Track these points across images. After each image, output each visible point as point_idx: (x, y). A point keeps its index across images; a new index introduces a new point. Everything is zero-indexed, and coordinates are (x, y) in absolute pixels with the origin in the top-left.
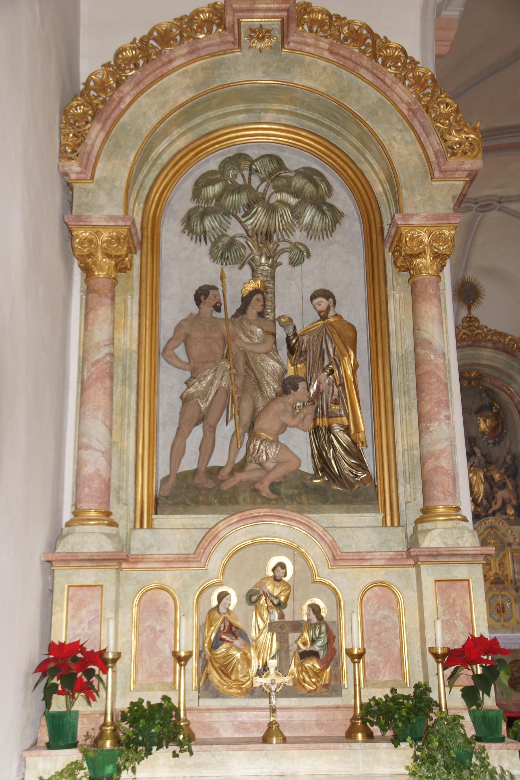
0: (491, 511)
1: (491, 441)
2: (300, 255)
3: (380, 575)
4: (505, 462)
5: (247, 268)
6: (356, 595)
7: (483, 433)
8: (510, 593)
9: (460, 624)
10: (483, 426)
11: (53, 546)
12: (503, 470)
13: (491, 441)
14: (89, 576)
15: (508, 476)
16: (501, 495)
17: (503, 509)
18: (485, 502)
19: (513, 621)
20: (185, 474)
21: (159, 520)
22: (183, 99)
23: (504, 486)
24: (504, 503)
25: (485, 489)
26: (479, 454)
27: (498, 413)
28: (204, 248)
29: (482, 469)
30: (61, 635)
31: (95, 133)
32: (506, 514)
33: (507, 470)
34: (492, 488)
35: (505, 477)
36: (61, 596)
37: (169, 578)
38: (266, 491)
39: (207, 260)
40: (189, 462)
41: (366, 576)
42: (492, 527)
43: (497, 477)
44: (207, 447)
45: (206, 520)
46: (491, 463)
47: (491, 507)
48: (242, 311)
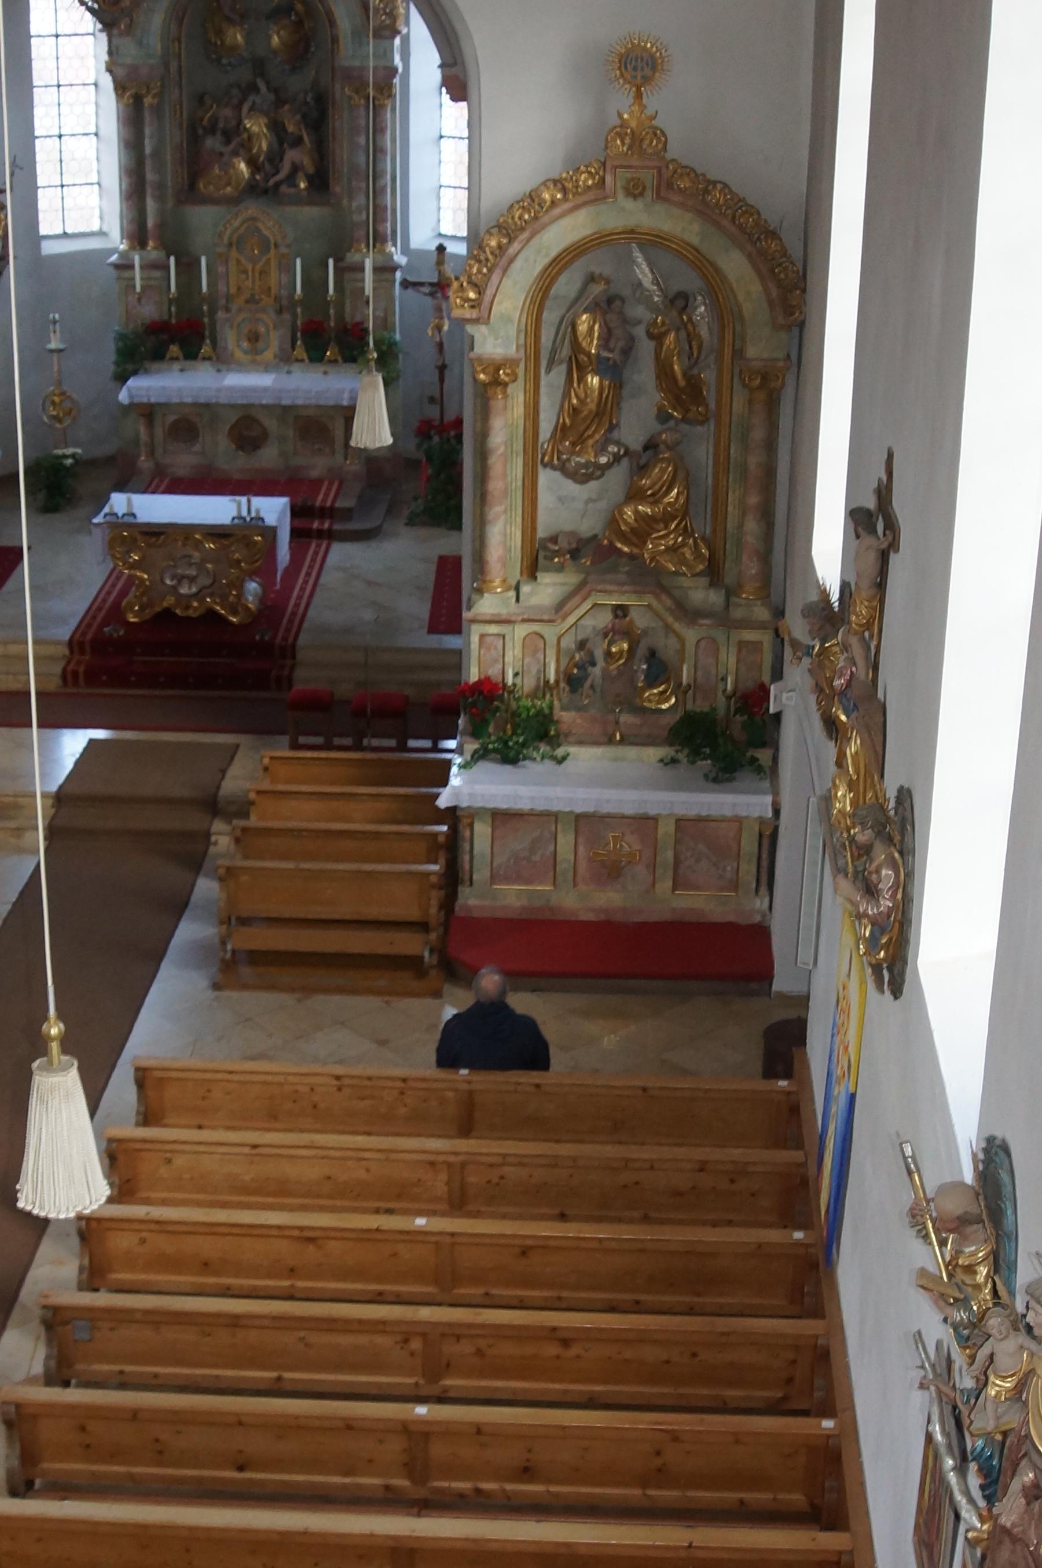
0: (271, 182)
1: (287, 67)
4: (306, 103)
7: (275, 53)
8: (269, 317)
10: (275, 40)
12: (298, 117)
13: (287, 67)
15: (306, 126)
16: (292, 155)
17: (291, 181)
18: (267, 166)
19: (269, 355)
23: (298, 142)
24: (295, 169)
25: (269, 146)
26: (263, 88)
27: (299, 24)
29: (266, 114)
32: (296, 186)
33: (304, 117)
34: (281, 143)
35: (302, 127)
42: (254, 219)
43: (291, 129)
46: (284, 103)
47: (277, 172)
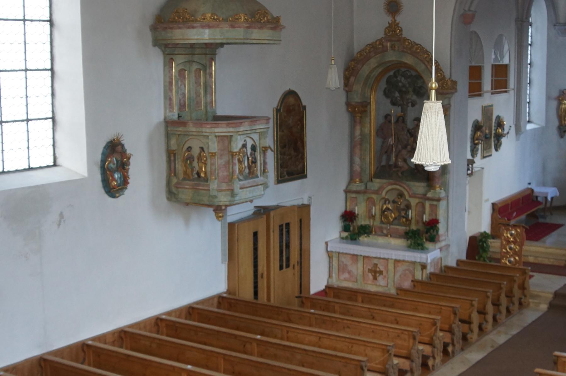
2: (413, 105)
3: (421, 200)
5: (400, 107)
6: (415, 205)
9: (434, 215)
11: (347, 187)
14: (354, 195)
20: (383, 166)
21: (374, 180)
22: (374, 66)
28: (389, 101)
30: (348, 210)
31: (352, 79)
36: (348, 200)
37: (374, 196)
38: (400, 174)
39: (390, 104)
40: (383, 163)
41: (417, 201)
44: (389, 159)
45: (384, 181)
48: (397, 121)
